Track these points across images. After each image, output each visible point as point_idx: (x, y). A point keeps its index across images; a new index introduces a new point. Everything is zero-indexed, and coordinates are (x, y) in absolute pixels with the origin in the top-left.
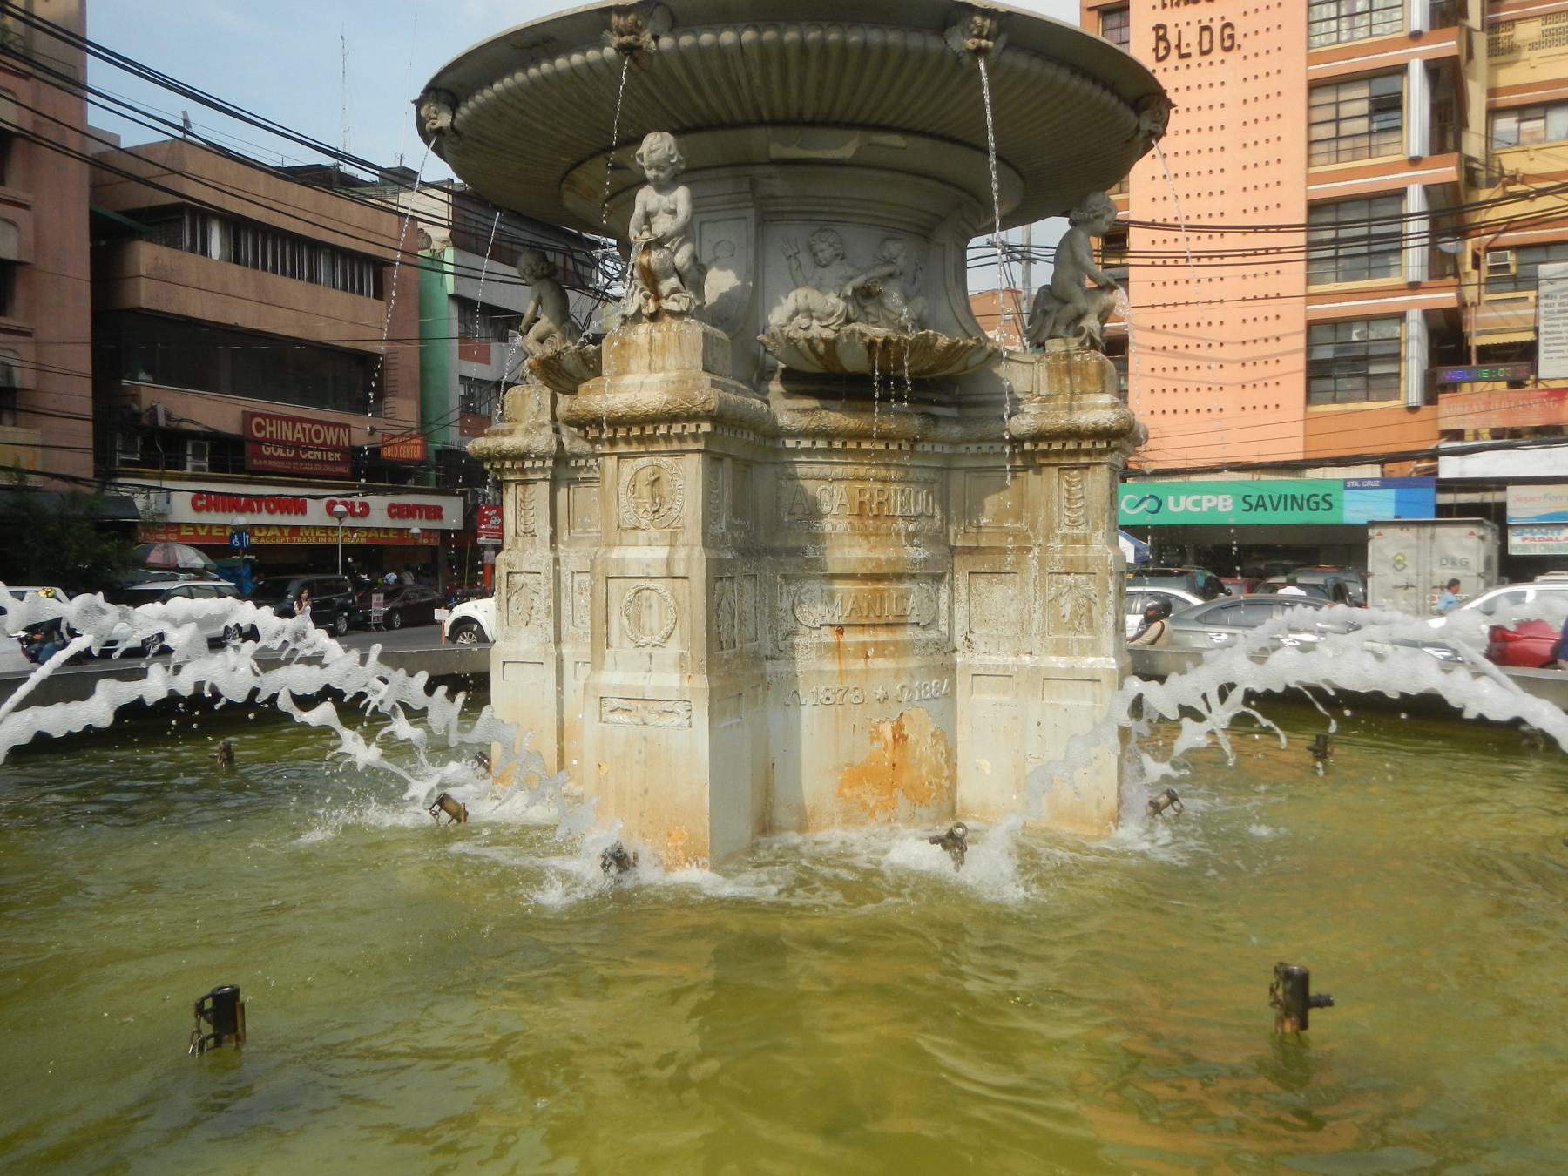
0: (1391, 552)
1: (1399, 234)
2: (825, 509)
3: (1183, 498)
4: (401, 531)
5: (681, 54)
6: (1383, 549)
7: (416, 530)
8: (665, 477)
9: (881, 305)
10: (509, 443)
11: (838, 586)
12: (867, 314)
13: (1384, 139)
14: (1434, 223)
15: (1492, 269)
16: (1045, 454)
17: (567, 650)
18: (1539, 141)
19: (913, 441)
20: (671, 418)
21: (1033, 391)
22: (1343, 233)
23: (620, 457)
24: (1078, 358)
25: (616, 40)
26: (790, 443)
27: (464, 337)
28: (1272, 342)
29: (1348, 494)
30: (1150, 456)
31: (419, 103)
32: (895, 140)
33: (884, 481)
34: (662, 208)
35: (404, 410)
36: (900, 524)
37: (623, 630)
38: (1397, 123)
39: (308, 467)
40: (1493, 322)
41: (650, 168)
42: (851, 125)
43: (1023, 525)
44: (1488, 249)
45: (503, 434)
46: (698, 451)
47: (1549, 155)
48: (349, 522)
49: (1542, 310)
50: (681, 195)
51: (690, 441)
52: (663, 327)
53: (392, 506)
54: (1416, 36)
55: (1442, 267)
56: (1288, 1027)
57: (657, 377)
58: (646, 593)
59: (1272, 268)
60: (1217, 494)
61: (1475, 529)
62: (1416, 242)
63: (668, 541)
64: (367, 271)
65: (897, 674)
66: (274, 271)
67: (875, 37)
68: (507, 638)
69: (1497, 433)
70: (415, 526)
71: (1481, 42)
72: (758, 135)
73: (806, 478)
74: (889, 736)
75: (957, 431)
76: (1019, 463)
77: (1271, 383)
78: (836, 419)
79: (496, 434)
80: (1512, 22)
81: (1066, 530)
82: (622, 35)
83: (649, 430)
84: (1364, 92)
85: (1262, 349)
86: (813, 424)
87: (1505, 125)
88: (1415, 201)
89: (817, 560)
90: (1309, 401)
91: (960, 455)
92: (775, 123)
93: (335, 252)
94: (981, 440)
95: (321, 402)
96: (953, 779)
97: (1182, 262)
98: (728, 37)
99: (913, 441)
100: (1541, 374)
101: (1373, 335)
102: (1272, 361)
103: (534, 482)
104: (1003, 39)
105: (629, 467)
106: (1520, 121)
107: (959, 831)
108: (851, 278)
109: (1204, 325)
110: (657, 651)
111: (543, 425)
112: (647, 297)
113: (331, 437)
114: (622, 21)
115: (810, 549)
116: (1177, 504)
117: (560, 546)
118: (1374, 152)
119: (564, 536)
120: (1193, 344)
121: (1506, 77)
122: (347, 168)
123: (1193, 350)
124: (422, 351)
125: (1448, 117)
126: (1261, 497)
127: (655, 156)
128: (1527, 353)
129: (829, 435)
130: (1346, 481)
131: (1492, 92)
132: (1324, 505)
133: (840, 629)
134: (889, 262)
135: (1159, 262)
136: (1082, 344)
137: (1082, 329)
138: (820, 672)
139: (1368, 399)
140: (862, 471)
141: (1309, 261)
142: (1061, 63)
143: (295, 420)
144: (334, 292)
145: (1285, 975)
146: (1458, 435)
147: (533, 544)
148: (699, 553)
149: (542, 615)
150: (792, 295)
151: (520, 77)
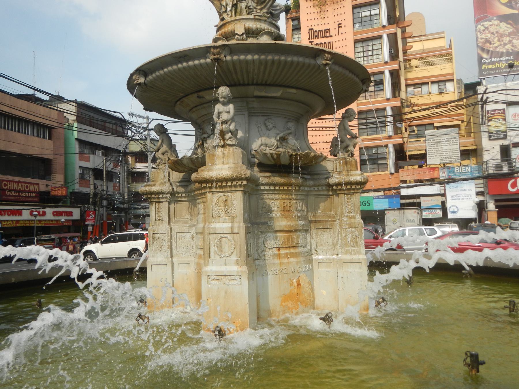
0: (392, 218)
1: (385, 121)
2: (273, 209)
4: (57, 220)
5: (233, 62)
6: (389, 217)
7: (63, 220)
8: (229, 199)
9: (287, 142)
10: (154, 189)
11: (278, 234)
12: (283, 145)
13: (379, 93)
14: (394, 118)
15: (410, 132)
16: (340, 190)
17: (175, 259)
18: (420, 94)
19: (299, 186)
20: (232, 179)
21: (335, 170)
22: (368, 121)
23: (213, 193)
24: (348, 160)
25: (212, 57)
26: (262, 188)
27: (80, 153)
29: (374, 200)
31: (132, 75)
32: (294, 91)
33: (290, 199)
34: (224, 112)
35: (58, 178)
36: (296, 213)
37: (215, 252)
38: (382, 88)
39: (23, 199)
40: (413, 147)
41: (222, 98)
42: (280, 86)
43: (333, 213)
44: (409, 126)
45: (151, 185)
46: (241, 191)
48: (38, 218)
49: (427, 144)
50: (231, 107)
51: (238, 187)
52: (227, 150)
53: (54, 212)
54: (386, 63)
55: (397, 131)
56: (474, 372)
57: (227, 166)
58: (223, 239)
61: (416, 211)
63: (231, 221)
64: (46, 130)
65: (297, 263)
66: (12, 130)
67: (295, 59)
68: (153, 256)
69: (416, 181)
70: (63, 219)
71: (402, 65)
72: (252, 88)
73: (267, 199)
74: (296, 284)
75: (311, 183)
76: (331, 193)
78: (277, 179)
79: (148, 186)
80: (410, 60)
81: (347, 214)
82: (215, 55)
83: (224, 184)
86: (270, 181)
87: (410, 89)
88: (389, 112)
89: (271, 226)
91: (311, 190)
92: (257, 84)
93: (35, 124)
94: (319, 186)
95: (28, 176)
96: (313, 297)
97: (321, 129)
98: (249, 57)
99: (299, 186)
100: (429, 162)
101: (379, 152)
103: (162, 202)
104: (332, 61)
105: (216, 196)
106: (414, 88)
107: (330, 315)
108: (278, 134)
110: (229, 258)
111: (165, 182)
112: (220, 140)
113: (32, 188)
114: (215, 51)
115: (269, 222)
117: (171, 224)
118: (376, 97)
119: (173, 220)
121: (410, 75)
122: (38, 95)
124: (66, 159)
125: (396, 86)
127: (224, 94)
128: (423, 157)
129: (274, 185)
131: (406, 80)
132: (367, 204)
133: (279, 249)
134: (289, 129)
135: (314, 129)
136: (349, 155)
137: (349, 150)
138: (274, 264)
139: (378, 171)
140: (284, 196)
141: (359, 129)
142: (347, 69)
143: (18, 182)
144: (34, 137)
145: (472, 356)
146: (405, 182)
147: (162, 223)
148: (242, 225)
149: (166, 248)
150: (260, 139)
151: (175, 67)
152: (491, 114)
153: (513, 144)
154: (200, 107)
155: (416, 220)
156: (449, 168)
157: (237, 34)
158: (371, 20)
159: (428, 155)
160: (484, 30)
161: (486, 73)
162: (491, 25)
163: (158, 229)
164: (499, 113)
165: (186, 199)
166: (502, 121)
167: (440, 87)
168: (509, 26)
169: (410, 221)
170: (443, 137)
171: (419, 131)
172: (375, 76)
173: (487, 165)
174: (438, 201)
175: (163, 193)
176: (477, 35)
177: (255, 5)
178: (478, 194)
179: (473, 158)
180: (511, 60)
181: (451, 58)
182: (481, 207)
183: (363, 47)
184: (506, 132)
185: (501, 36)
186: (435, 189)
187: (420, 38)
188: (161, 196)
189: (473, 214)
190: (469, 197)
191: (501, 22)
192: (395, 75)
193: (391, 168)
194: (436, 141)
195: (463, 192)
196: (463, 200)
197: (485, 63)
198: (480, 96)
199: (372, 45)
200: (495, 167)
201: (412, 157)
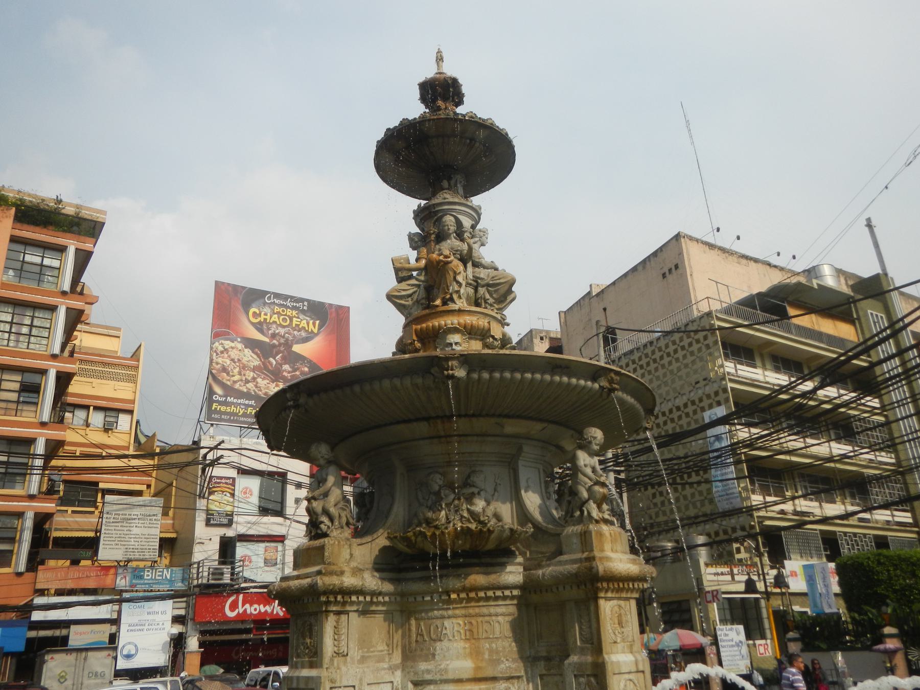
1: (26, 464)
8: (622, 611)
13: (25, 408)
25: (604, 383)
40: (70, 522)
47: (116, 437)
54: (54, 357)
62: (38, 472)
84: (19, 378)
88: (40, 448)
103: (347, 613)
118: (19, 414)
125: (62, 404)
128: (91, 545)
147: (345, 662)
151: (548, 377)
154: (475, 438)
156: (136, 569)
157: (493, 337)
158: (40, 274)
160: (222, 352)
161: (216, 416)
162: (232, 348)
163: (341, 677)
164: (226, 483)
165: (384, 608)
166: (228, 498)
167: (108, 419)
168: (255, 357)
170: (137, 512)
171: (82, 492)
172: (26, 374)
174: (102, 633)
175: (360, 592)
176: (211, 356)
177: (491, 301)
178: (177, 620)
179: (166, 555)
180: (251, 406)
181: (136, 376)
182: (178, 642)
183: (13, 314)
184: (232, 515)
185: (244, 367)
187: (105, 331)
188: (354, 598)
191: (246, 347)
192: (64, 379)
193: (21, 560)
194: (121, 516)
195: (151, 617)
197: (217, 401)
198: (203, 452)
199: (33, 317)
200: (213, 574)
201: (59, 542)
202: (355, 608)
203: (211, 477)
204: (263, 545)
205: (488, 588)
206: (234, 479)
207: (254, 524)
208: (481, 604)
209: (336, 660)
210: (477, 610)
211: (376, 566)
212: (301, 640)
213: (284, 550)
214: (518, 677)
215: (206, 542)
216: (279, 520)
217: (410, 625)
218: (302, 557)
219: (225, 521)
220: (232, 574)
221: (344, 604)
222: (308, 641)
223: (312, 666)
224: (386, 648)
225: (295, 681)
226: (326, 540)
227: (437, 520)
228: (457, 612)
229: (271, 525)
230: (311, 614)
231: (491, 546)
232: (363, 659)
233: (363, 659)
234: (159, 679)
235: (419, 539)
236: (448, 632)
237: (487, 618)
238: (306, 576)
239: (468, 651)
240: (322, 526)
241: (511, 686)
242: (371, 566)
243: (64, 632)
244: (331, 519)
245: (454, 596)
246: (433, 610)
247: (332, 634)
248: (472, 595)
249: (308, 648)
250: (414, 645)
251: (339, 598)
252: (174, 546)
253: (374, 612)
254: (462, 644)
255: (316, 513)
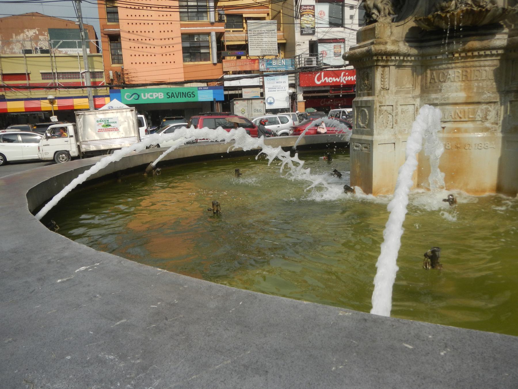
0: (241, 109)
1: (206, 6)
3: (146, 94)
28: (171, 39)
29: (199, 91)
30: (133, 79)
40: (233, 37)
59: (169, 14)
60: (158, 92)
69: (234, 73)
77: (172, 54)
85: (167, 42)
90: (184, 61)
101: (201, 40)
102: (171, 46)
103: (389, 66)
109: (147, 32)
116: (145, 96)
120: (144, 39)
123: (144, 41)
126: (172, 93)
128: (244, 48)
130: (198, 87)
132: (192, 96)
139: (201, 61)
141: (180, 12)
146: (226, 73)
147: (388, 93)
152: (304, 9)
153: (319, 40)
155: (262, 109)
159: (249, 47)
164: (310, 9)
165: (411, 64)
169: (258, 111)
170: (264, 29)
171: (236, 20)
173: (299, 58)
174: (257, 92)
178: (291, 86)
182: (293, 97)
184: (314, 28)
186: (255, 81)
188: (393, 58)
189: (286, 105)
190: (283, 89)
195: (278, 84)
196: (279, 91)
200: (307, 61)
201: (230, 48)
202: (393, 63)
203: (301, 6)
204: (333, 44)
205: (481, 50)
206: (314, 6)
207: (327, 32)
208: (474, 59)
209: (382, 92)
210: (472, 63)
211: (407, 39)
212: (362, 82)
213: (345, 47)
214: (495, 102)
215: (302, 44)
216: (341, 29)
217: (426, 73)
218: (361, 36)
219: (311, 32)
220: (317, 62)
221: (387, 61)
222: (366, 82)
223: (369, 95)
224: (411, 86)
225: (360, 103)
226: (376, 24)
227: (449, 7)
228: (458, 65)
229: (337, 32)
230: (367, 68)
231: (486, 21)
232: (397, 92)
233: (397, 92)
234: (286, 113)
235: (436, 19)
236: (451, 77)
237: (478, 68)
238: (365, 46)
239: (463, 87)
240: (374, 16)
241: (489, 107)
242: (403, 39)
243: (240, 92)
244: (379, 12)
245: (457, 55)
246: (442, 64)
247: (380, 77)
248: (469, 54)
249: (366, 86)
250: (428, 84)
251: (384, 58)
252: (285, 47)
253: (405, 66)
254: (459, 84)
255: (369, 8)
